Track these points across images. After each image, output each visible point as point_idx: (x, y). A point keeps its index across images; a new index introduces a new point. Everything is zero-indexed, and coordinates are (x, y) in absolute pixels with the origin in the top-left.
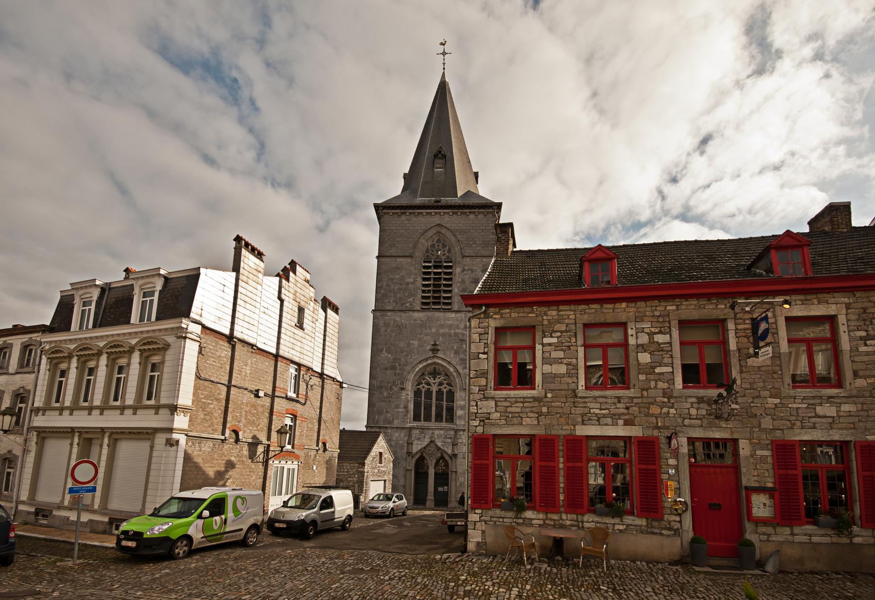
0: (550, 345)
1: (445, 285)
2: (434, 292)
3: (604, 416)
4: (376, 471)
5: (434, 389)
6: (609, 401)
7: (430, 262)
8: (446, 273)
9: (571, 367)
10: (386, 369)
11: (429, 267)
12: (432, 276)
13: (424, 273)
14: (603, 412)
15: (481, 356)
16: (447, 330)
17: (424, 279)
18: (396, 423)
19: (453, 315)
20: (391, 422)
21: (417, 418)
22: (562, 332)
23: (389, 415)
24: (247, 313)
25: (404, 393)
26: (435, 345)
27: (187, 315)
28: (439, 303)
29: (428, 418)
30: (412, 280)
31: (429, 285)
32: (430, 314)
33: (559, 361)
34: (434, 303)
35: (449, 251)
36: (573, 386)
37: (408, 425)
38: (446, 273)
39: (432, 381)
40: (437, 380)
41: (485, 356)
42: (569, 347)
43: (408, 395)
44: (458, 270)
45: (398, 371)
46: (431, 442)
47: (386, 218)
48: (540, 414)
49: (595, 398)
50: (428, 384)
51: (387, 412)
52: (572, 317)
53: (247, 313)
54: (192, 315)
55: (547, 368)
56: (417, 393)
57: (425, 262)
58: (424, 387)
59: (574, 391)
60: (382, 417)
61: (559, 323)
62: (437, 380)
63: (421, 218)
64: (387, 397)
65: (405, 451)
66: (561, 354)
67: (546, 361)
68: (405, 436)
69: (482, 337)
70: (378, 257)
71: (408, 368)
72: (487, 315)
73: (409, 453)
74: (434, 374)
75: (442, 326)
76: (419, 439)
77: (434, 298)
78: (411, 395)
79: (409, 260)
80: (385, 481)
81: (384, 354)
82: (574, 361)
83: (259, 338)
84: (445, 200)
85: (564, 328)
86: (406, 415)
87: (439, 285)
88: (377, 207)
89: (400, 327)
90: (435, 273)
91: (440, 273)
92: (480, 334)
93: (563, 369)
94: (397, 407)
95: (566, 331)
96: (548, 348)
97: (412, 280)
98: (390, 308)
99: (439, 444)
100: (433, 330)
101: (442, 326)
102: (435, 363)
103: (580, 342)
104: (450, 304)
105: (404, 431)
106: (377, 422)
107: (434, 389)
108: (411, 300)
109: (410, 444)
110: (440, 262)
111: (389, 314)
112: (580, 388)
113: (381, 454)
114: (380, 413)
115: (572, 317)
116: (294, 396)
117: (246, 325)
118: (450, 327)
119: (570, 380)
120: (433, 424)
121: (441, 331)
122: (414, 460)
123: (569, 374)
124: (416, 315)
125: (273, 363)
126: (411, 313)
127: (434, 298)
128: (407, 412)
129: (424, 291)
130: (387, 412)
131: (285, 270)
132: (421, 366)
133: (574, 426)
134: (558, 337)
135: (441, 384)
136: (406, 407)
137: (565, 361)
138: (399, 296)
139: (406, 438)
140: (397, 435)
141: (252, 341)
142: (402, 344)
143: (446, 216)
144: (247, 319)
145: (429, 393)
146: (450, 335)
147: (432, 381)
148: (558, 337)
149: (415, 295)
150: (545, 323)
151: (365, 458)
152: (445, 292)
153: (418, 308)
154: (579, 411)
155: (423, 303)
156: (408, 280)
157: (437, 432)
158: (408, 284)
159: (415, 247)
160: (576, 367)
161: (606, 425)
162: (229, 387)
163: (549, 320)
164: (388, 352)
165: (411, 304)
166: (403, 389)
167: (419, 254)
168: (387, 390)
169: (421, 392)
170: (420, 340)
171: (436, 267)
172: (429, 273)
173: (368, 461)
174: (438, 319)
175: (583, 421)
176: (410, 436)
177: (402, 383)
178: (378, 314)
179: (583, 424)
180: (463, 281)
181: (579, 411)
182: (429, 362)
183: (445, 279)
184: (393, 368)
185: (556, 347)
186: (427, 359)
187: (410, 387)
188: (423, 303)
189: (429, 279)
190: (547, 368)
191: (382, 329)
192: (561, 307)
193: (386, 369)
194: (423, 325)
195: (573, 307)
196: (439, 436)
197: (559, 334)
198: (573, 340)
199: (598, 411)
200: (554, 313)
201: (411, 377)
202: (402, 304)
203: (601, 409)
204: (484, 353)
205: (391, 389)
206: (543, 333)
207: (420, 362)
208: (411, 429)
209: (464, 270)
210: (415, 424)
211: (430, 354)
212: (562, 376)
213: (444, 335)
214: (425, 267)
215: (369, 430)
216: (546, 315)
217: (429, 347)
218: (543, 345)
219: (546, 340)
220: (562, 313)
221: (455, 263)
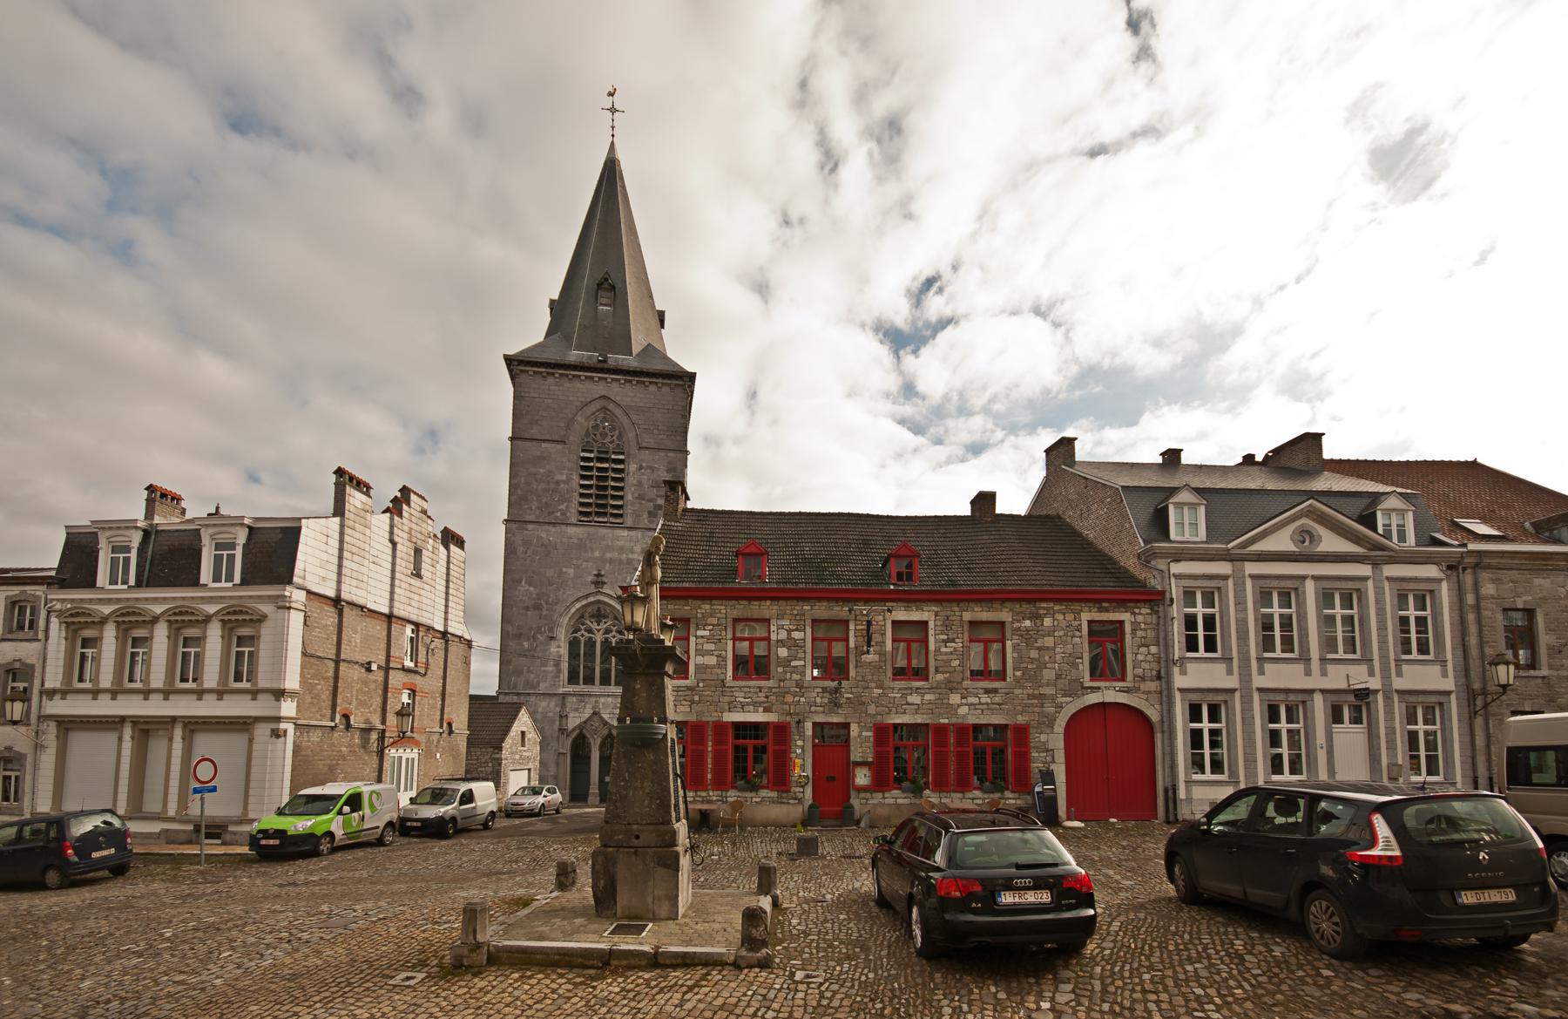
2: (598, 497)
5: (599, 638)
10: (527, 609)
11: (590, 460)
12: (595, 473)
13: (583, 468)
16: (616, 555)
17: (583, 477)
18: (543, 687)
19: (625, 533)
20: (536, 686)
21: (573, 678)
24: (355, 566)
25: (554, 643)
26: (599, 575)
27: (290, 582)
28: (605, 514)
29: (589, 680)
31: (590, 487)
32: (592, 530)
33: (710, 653)
34: (598, 514)
35: (620, 437)
37: (561, 690)
38: (615, 470)
39: (594, 626)
40: (603, 626)
43: (560, 649)
44: (633, 467)
46: (595, 713)
47: (523, 378)
48: (692, 702)
50: (590, 631)
51: (529, 671)
53: (355, 566)
54: (295, 579)
55: (700, 660)
56: (573, 644)
58: (583, 636)
60: (522, 680)
62: (603, 626)
63: (577, 384)
65: (556, 727)
66: (712, 647)
67: (700, 652)
70: (512, 439)
71: (560, 608)
73: (562, 731)
74: (599, 616)
75: (608, 548)
76: (576, 710)
77: (598, 505)
78: (564, 651)
79: (560, 447)
81: (524, 587)
83: (370, 597)
84: (615, 359)
87: (605, 488)
88: (509, 360)
89: (547, 548)
90: (599, 469)
91: (606, 470)
93: (713, 660)
98: (532, 518)
99: (606, 717)
100: (597, 554)
101: (608, 548)
102: (599, 602)
103: (730, 636)
104: (621, 516)
107: (599, 638)
108: (563, 507)
109: (563, 717)
111: (530, 527)
114: (519, 673)
116: (412, 665)
117: (354, 583)
118: (621, 550)
120: (596, 689)
121: (608, 555)
122: (570, 740)
123: (719, 666)
124: (571, 530)
125: (385, 626)
127: (598, 505)
128: (559, 671)
129: (582, 495)
130: (529, 671)
131: (395, 500)
132: (578, 605)
135: (607, 631)
136: (557, 664)
140: (544, 704)
141: (361, 602)
142: (550, 573)
143: (615, 384)
144: (355, 575)
145: (591, 644)
146: (620, 561)
147: (594, 626)
149: (569, 501)
151: (503, 740)
152: (614, 497)
153: (574, 520)
154: (726, 699)
155: (581, 513)
156: (558, 477)
157: (602, 700)
158: (558, 483)
159: (568, 427)
160: (725, 659)
162: (337, 662)
166: (552, 638)
167: (575, 439)
169: (579, 642)
170: (577, 567)
171: (600, 460)
172: (590, 469)
173: (507, 744)
174: (603, 538)
176: (563, 705)
177: (551, 630)
178: (514, 526)
180: (640, 484)
181: (726, 699)
182: (591, 599)
183: (614, 479)
184: (538, 607)
185: (709, 639)
186: (587, 596)
187: (562, 635)
189: (589, 478)
190: (700, 660)
191: (520, 550)
193: (527, 609)
194: (581, 546)
196: (606, 706)
201: (565, 620)
205: (534, 637)
207: (578, 600)
208: (564, 696)
209: (641, 468)
210: (570, 689)
211: (592, 589)
212: (713, 667)
213: (611, 561)
214: (584, 459)
217: (590, 578)
219: (700, 633)
221: (629, 456)
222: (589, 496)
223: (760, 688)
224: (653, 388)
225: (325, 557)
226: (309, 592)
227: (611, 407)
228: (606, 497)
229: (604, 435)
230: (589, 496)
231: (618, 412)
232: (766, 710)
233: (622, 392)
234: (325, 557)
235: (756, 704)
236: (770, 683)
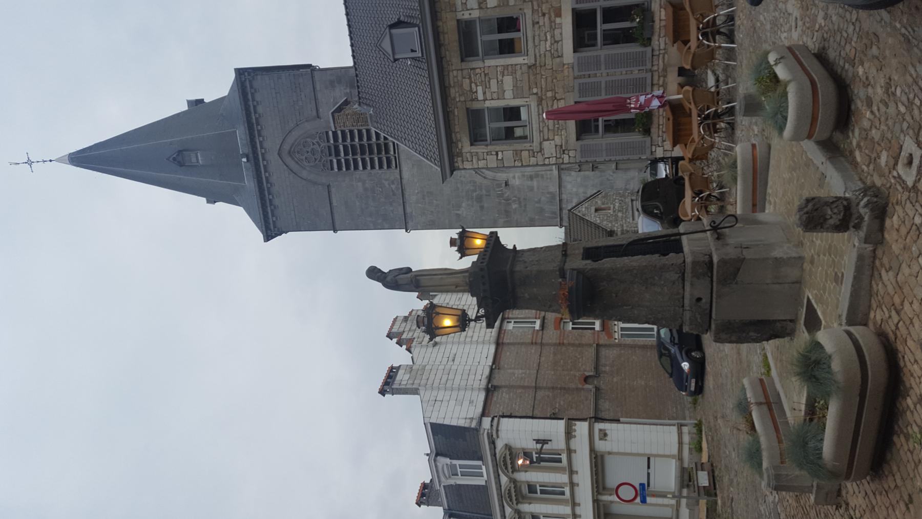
0: (484, 93)
1: (361, 139)
2: (371, 153)
3: (553, 36)
4: (620, 214)
6: (537, 33)
7: (331, 161)
8: (344, 139)
9: (506, 72)
10: (482, 208)
11: (339, 162)
12: (350, 157)
13: (348, 168)
14: (549, 37)
15: (500, 157)
17: (356, 168)
18: (554, 188)
20: (553, 195)
22: (471, 82)
23: (543, 199)
30: (360, 184)
31: (363, 161)
33: (500, 83)
34: (387, 152)
36: (525, 68)
38: (344, 139)
41: (500, 154)
42: (485, 75)
45: (484, 192)
49: (535, 46)
51: (539, 202)
52: (455, 73)
55: (509, 94)
57: (332, 169)
59: (529, 67)
61: (462, 85)
64: (520, 203)
66: (493, 82)
67: (501, 96)
68: (570, 175)
69: (481, 158)
72: (460, 154)
77: (379, 152)
79: (333, 190)
80: (632, 200)
82: (499, 69)
85: (467, 81)
86: (542, 176)
87: (362, 146)
90: (346, 154)
91: (345, 147)
92: (478, 159)
93: (508, 81)
94: (531, 189)
95: (470, 78)
96: (488, 96)
97: (360, 184)
98: (401, 209)
105: (564, 177)
106: (554, 213)
108: (386, 183)
110: (329, 147)
111: (408, 210)
112: (526, 62)
113: (596, 210)
114: (541, 211)
115: (455, 73)
116: (538, 322)
119: (519, 73)
123: (513, 73)
124: (406, 175)
126: (404, 182)
127: (379, 152)
129: (373, 167)
130: (539, 202)
133: (564, 65)
134: (477, 86)
136: (531, 178)
137: (500, 78)
138: (383, 200)
139: (573, 173)
140: (569, 186)
148: (477, 86)
150: (462, 99)
153: (398, 171)
155: (389, 166)
158: (366, 189)
160: (506, 67)
161: (561, 34)
163: (460, 95)
164: (459, 206)
165: (393, 183)
166: (507, 184)
168: (509, 204)
171: (337, 154)
172: (347, 161)
175: (559, 57)
178: (410, 224)
179: (562, 56)
181: (549, 61)
183: (352, 139)
184: (479, 199)
185: (486, 86)
188: (389, 166)
189: (355, 161)
190: (509, 94)
192: (447, 84)
193: (482, 208)
195: (446, 73)
197: (473, 85)
198: (478, 71)
199: (548, 43)
200: (452, 91)
202: (394, 194)
203: (546, 40)
204: (497, 154)
205: (507, 200)
206: (472, 100)
212: (515, 80)
214: (340, 168)
215: (565, 223)
216: (455, 98)
218: (485, 100)
219: (481, 97)
220: (452, 83)
222: (372, 160)
223: (535, 23)
224: (260, 109)
225: (452, 403)
226: (483, 414)
227: (286, 147)
228: (370, 145)
229: (313, 152)
230: (372, 160)
231: (290, 140)
232: (559, 14)
233: (271, 140)
234: (452, 403)
235: (553, 27)
236: (528, 12)
